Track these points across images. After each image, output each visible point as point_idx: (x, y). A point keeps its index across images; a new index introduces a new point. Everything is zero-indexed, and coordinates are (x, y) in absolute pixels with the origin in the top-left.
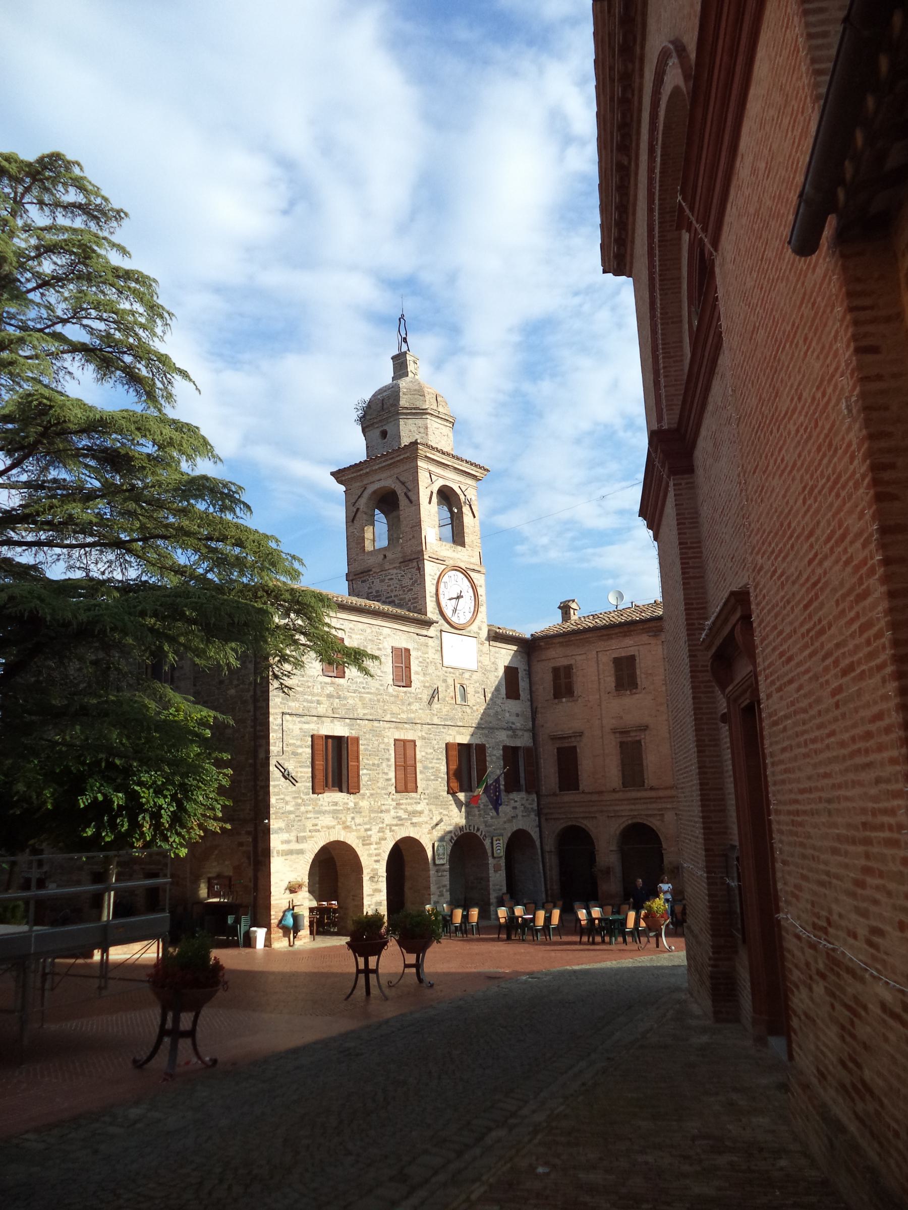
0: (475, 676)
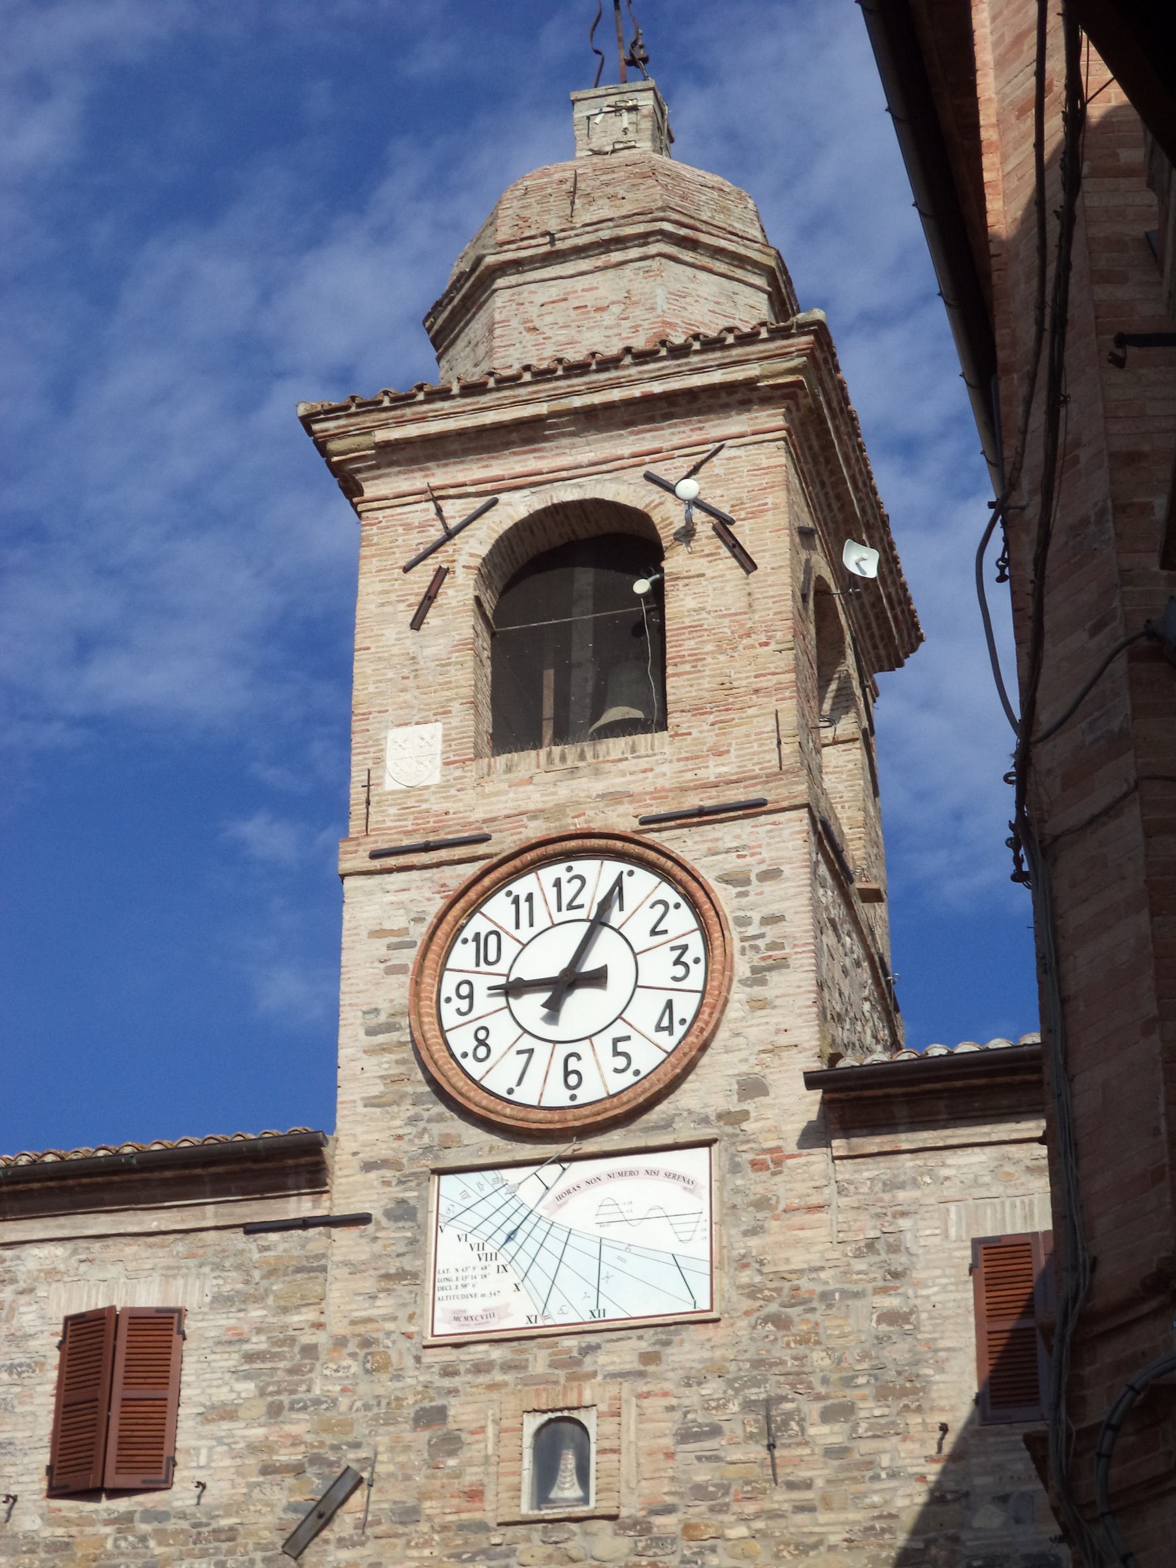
0: (688, 1351)
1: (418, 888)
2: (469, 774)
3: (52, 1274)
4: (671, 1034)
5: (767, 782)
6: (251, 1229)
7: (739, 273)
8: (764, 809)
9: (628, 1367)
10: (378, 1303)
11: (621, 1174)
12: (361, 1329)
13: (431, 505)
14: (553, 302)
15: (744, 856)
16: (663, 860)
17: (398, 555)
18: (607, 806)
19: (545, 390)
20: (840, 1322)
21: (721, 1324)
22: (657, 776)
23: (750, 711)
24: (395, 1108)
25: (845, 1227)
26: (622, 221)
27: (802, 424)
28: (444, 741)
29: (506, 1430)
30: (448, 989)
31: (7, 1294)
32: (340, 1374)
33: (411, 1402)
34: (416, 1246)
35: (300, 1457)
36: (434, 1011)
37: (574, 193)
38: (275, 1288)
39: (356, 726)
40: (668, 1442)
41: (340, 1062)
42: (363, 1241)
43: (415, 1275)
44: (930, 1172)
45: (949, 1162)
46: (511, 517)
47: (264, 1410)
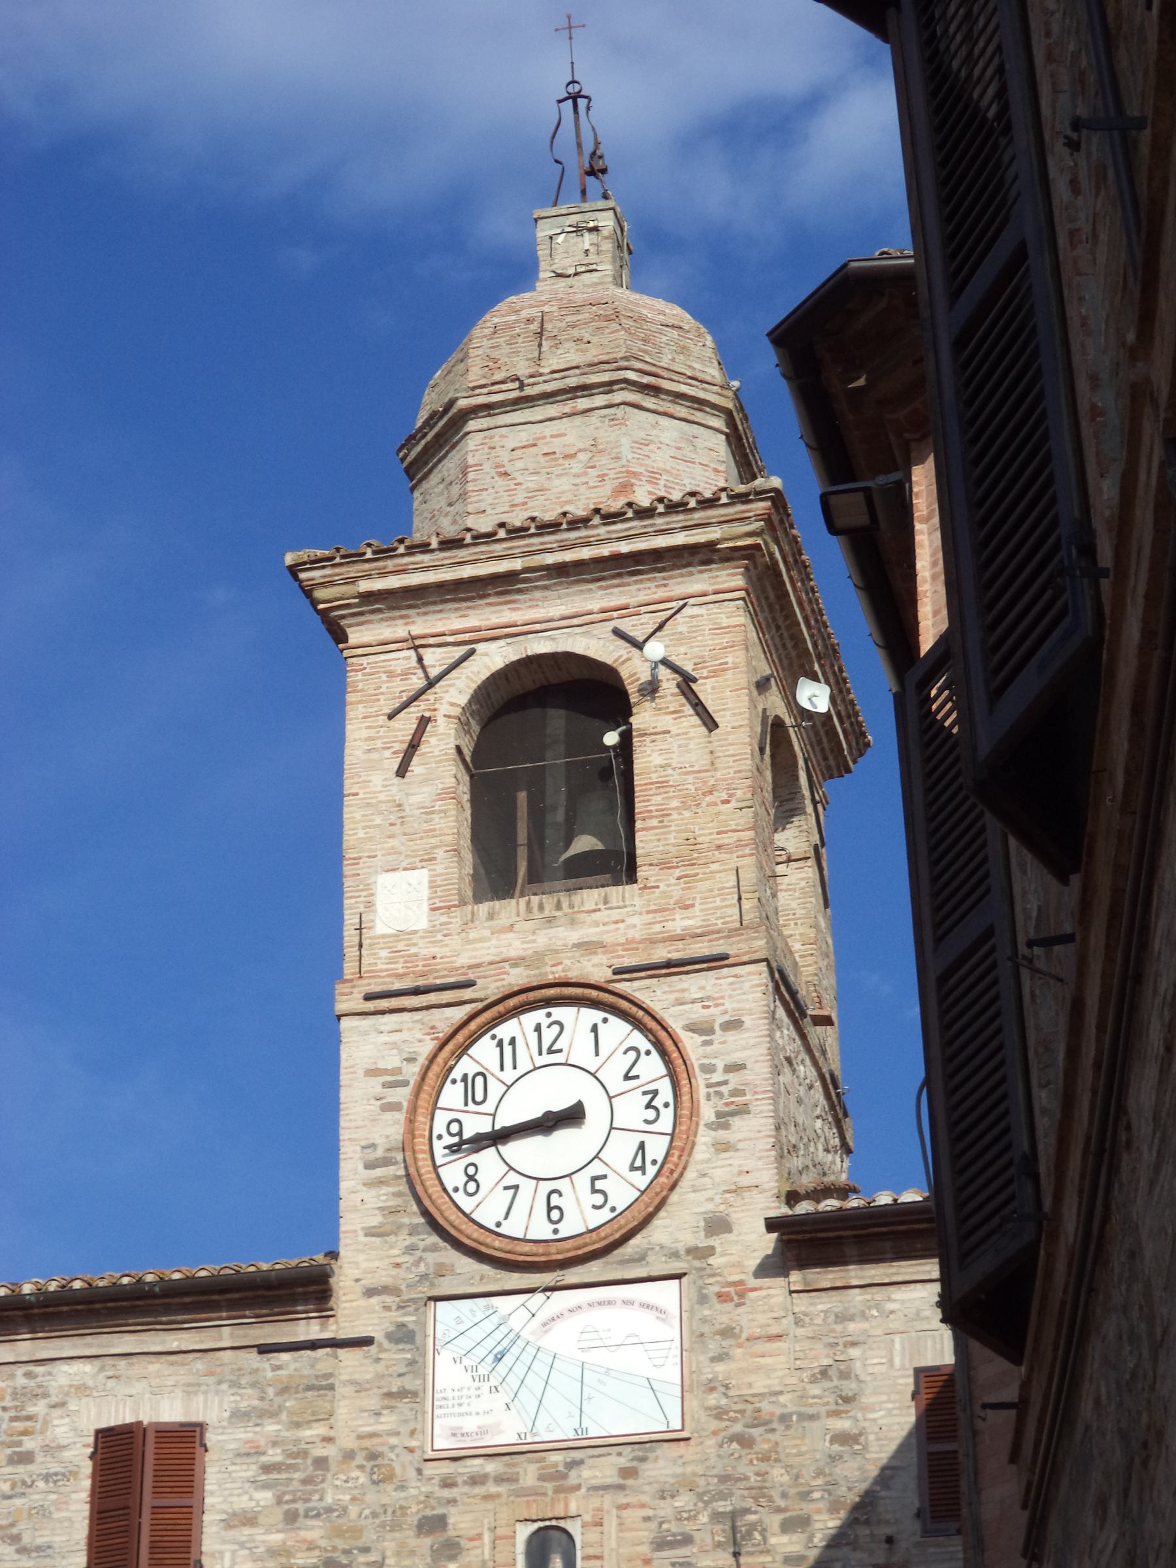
0: (662, 1467)
1: (409, 1029)
2: (454, 920)
3: (82, 1390)
4: (644, 1173)
5: (729, 937)
6: (264, 1349)
7: (699, 416)
8: (726, 962)
9: (609, 1481)
10: (383, 1419)
11: (600, 1304)
12: (367, 1443)
13: (412, 653)
14: (523, 447)
15: (709, 1007)
16: (634, 1009)
17: (382, 702)
18: (583, 955)
19: (519, 547)
20: (797, 1442)
21: (692, 1442)
22: (628, 927)
23: (714, 867)
24: (393, 1238)
25: (801, 1355)
26: (588, 369)
27: (760, 579)
28: (431, 887)
29: (501, 1538)
30: (439, 1127)
31: (39, 1408)
32: (349, 1485)
33: (414, 1510)
34: (416, 1366)
35: (315, 1560)
36: (427, 1148)
37: (541, 334)
38: (288, 1404)
39: (347, 870)
40: (645, 1549)
41: (342, 1193)
42: (367, 1361)
43: (415, 1394)
44: (877, 1307)
45: (894, 1297)
46: (488, 668)
47: (281, 1517)
